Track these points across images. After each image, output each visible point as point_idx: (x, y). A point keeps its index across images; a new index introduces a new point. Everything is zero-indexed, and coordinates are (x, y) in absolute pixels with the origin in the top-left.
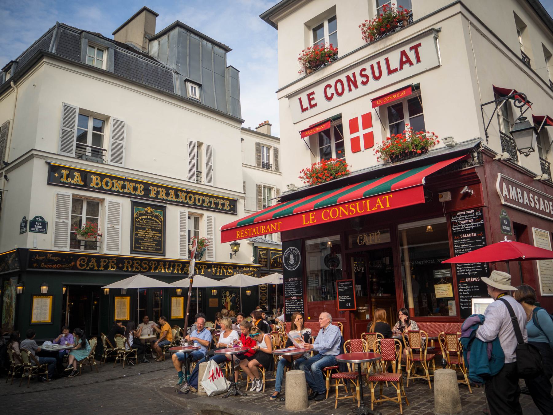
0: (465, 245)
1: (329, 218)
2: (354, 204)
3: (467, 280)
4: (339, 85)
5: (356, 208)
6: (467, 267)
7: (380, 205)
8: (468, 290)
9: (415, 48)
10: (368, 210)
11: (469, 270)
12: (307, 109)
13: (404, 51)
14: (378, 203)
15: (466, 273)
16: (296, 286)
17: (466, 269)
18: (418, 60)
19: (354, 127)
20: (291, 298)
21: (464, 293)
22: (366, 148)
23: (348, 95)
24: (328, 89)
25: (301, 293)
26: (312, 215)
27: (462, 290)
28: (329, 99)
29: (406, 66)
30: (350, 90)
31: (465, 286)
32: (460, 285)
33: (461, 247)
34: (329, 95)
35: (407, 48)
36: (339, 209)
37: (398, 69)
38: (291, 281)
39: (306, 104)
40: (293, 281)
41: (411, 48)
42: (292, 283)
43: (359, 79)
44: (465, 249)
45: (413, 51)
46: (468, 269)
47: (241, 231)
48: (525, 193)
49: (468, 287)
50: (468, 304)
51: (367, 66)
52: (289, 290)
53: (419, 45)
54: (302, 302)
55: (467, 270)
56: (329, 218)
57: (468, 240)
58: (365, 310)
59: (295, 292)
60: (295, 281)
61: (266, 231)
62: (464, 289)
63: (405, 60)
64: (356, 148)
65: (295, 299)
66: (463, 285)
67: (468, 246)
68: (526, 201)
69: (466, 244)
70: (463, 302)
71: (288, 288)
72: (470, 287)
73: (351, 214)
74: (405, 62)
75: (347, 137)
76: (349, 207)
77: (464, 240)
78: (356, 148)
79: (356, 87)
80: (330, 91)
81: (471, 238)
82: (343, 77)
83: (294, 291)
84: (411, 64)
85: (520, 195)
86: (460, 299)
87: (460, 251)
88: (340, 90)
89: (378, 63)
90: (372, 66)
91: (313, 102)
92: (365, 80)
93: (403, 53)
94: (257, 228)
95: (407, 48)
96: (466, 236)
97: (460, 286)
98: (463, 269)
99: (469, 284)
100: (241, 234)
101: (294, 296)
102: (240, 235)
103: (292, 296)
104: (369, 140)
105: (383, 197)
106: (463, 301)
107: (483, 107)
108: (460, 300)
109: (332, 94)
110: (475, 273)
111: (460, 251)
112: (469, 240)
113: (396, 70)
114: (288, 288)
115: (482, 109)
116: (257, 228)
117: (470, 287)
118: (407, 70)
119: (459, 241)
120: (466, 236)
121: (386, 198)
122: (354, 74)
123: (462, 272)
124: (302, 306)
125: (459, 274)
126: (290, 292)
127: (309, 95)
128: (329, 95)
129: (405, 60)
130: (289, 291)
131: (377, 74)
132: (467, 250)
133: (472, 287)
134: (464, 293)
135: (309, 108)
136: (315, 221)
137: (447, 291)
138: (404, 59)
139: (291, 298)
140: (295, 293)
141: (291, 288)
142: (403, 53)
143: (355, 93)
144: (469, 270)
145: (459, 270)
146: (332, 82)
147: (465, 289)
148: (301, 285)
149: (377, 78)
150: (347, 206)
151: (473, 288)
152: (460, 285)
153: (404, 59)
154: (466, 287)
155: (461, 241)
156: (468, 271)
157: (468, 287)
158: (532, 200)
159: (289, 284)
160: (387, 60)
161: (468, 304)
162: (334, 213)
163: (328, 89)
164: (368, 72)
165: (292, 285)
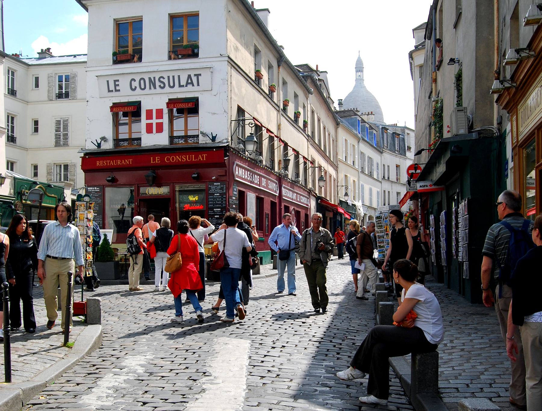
4: (142, 82)
9: (198, 76)
12: (112, 91)
13: (190, 75)
18: (198, 85)
19: (149, 114)
22: (157, 132)
23: (147, 91)
24: (133, 82)
29: (190, 86)
30: (150, 88)
34: (133, 87)
37: (185, 86)
41: (195, 75)
43: (158, 84)
45: (196, 77)
53: (200, 75)
63: (190, 82)
68: (246, 177)
74: (190, 83)
79: (155, 88)
84: (193, 85)
85: (243, 173)
88: (143, 87)
89: (173, 77)
90: (169, 77)
91: (118, 88)
92: (162, 85)
93: (189, 76)
104: (160, 128)
107: (232, 122)
109: (136, 87)
113: (183, 86)
115: (231, 123)
122: (154, 78)
127: (115, 81)
128: (133, 87)
129: (190, 82)
131: (172, 84)
135: (114, 91)
138: (189, 81)
142: (189, 76)
143: (153, 91)
153: (189, 81)
160: (179, 76)
163: (133, 82)
164: (166, 81)
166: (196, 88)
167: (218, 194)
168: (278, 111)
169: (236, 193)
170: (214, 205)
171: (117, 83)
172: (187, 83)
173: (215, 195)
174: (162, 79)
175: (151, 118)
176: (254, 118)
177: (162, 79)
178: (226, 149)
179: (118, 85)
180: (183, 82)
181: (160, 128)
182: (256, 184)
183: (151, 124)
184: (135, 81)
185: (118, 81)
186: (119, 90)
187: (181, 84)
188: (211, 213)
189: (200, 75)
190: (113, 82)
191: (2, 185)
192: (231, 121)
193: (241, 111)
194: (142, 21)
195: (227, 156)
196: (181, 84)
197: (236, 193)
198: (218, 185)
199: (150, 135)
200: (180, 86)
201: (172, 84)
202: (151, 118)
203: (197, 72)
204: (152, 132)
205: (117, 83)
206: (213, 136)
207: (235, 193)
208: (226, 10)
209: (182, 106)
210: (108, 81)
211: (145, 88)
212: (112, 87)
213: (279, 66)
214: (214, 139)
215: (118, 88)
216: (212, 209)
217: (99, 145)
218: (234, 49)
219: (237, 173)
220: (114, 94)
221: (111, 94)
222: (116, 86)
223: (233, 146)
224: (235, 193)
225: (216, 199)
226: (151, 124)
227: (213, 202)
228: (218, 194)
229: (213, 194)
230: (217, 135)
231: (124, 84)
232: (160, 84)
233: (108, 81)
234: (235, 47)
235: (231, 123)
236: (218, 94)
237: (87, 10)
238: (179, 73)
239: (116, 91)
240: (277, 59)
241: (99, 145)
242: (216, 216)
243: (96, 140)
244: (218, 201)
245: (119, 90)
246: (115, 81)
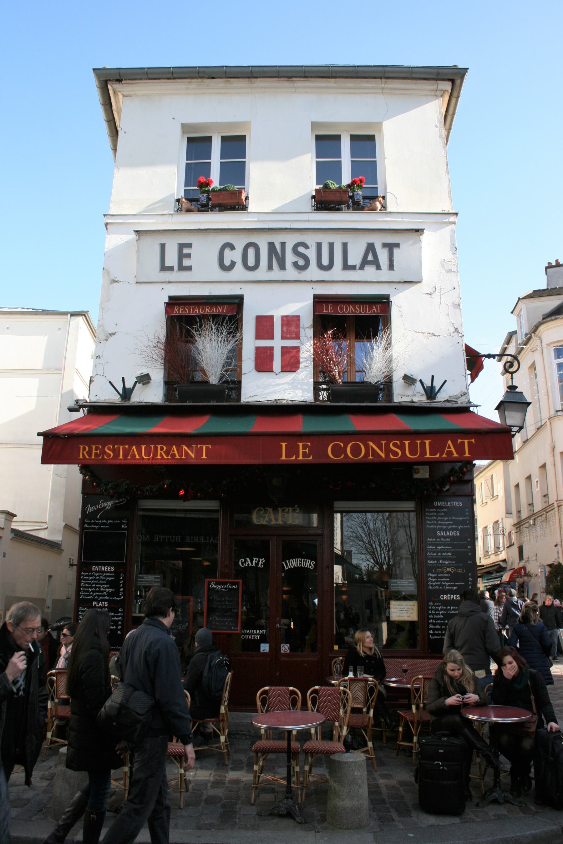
0: (442, 547)
1: (343, 456)
2: (398, 442)
3: (442, 597)
4: (251, 252)
5: (403, 450)
6: (444, 579)
7: (452, 451)
8: (443, 612)
9: (391, 247)
10: (428, 455)
11: (445, 583)
12: (171, 269)
14: (449, 447)
15: (441, 588)
16: (108, 582)
17: (441, 581)
20: (94, 603)
21: (435, 616)
23: (262, 273)
24: (227, 251)
25: (120, 597)
26: (304, 447)
27: (433, 612)
30: (270, 267)
31: (439, 606)
32: (431, 604)
33: (436, 548)
34: (227, 263)
36: (367, 446)
37: (358, 267)
38: (96, 572)
39: (172, 259)
40: (104, 572)
41: (385, 245)
42: (99, 576)
43: (290, 258)
44: (442, 552)
46: (444, 581)
47: (94, 447)
49: (442, 607)
50: (440, 632)
52: (91, 587)
54: (120, 614)
55: (443, 583)
56: (343, 456)
57: (448, 540)
58: (258, 634)
59: (105, 593)
60: (108, 572)
61: (167, 456)
62: (435, 610)
65: (105, 607)
66: (435, 604)
67: (448, 549)
69: (444, 545)
70: (434, 630)
71: (89, 584)
72: (445, 608)
73: (392, 456)
74: (370, 263)
76: (387, 445)
77: (442, 539)
79: (282, 267)
80: (229, 256)
81: (453, 538)
82: (263, 243)
83: (102, 592)
84: (379, 268)
86: (429, 624)
87: (435, 554)
88: (251, 261)
90: (319, 246)
92: (301, 262)
93: (371, 247)
94: (143, 447)
96: (446, 534)
97: (430, 605)
98: (437, 581)
99: (446, 603)
100: (94, 452)
101: (102, 600)
102: (90, 453)
103: (96, 600)
105: (459, 441)
106: (433, 627)
108: (428, 626)
109: (233, 264)
110: (455, 588)
111: (435, 554)
112: (449, 540)
113: (353, 268)
114: (89, 584)
116: (143, 447)
117: (445, 608)
118: (370, 272)
119: (434, 540)
120: (446, 534)
121: (464, 442)
122: (283, 245)
123: (436, 585)
124: (119, 620)
125: (430, 588)
126: (93, 592)
128: (227, 263)
130: (91, 590)
132: (446, 554)
133: (449, 608)
134: (435, 616)
135: (176, 268)
136: (311, 458)
137: (409, 612)
138: (370, 258)
139: (94, 603)
140: (104, 596)
141: (96, 584)
142: (371, 247)
143: (276, 274)
144: (445, 583)
145: (432, 581)
147: (438, 610)
148: (122, 582)
149: (320, 266)
150: (383, 442)
151: (450, 609)
152: (431, 604)
153: (370, 258)
154: (440, 608)
155: (438, 540)
156: (445, 585)
157: (442, 607)
159: (91, 576)
160: (345, 246)
161: (440, 632)
162: (356, 450)
163: (227, 251)
165: (99, 580)
166: (385, 274)
171: (186, 251)
172: (364, 263)
174: (301, 249)
179: (189, 256)
180: (355, 258)
184: (232, 247)
185: (190, 245)
186: (189, 268)
187: (350, 263)
196: (350, 263)
200: (346, 266)
201: (325, 261)
203: (391, 239)
204: (271, 370)
205: (186, 251)
209: (356, 309)
210: (163, 246)
211: (256, 266)
215: (186, 262)
220: (176, 275)
221: (168, 276)
232: (295, 259)
233: (163, 246)
239: (182, 268)
245: (189, 268)
246: (182, 246)
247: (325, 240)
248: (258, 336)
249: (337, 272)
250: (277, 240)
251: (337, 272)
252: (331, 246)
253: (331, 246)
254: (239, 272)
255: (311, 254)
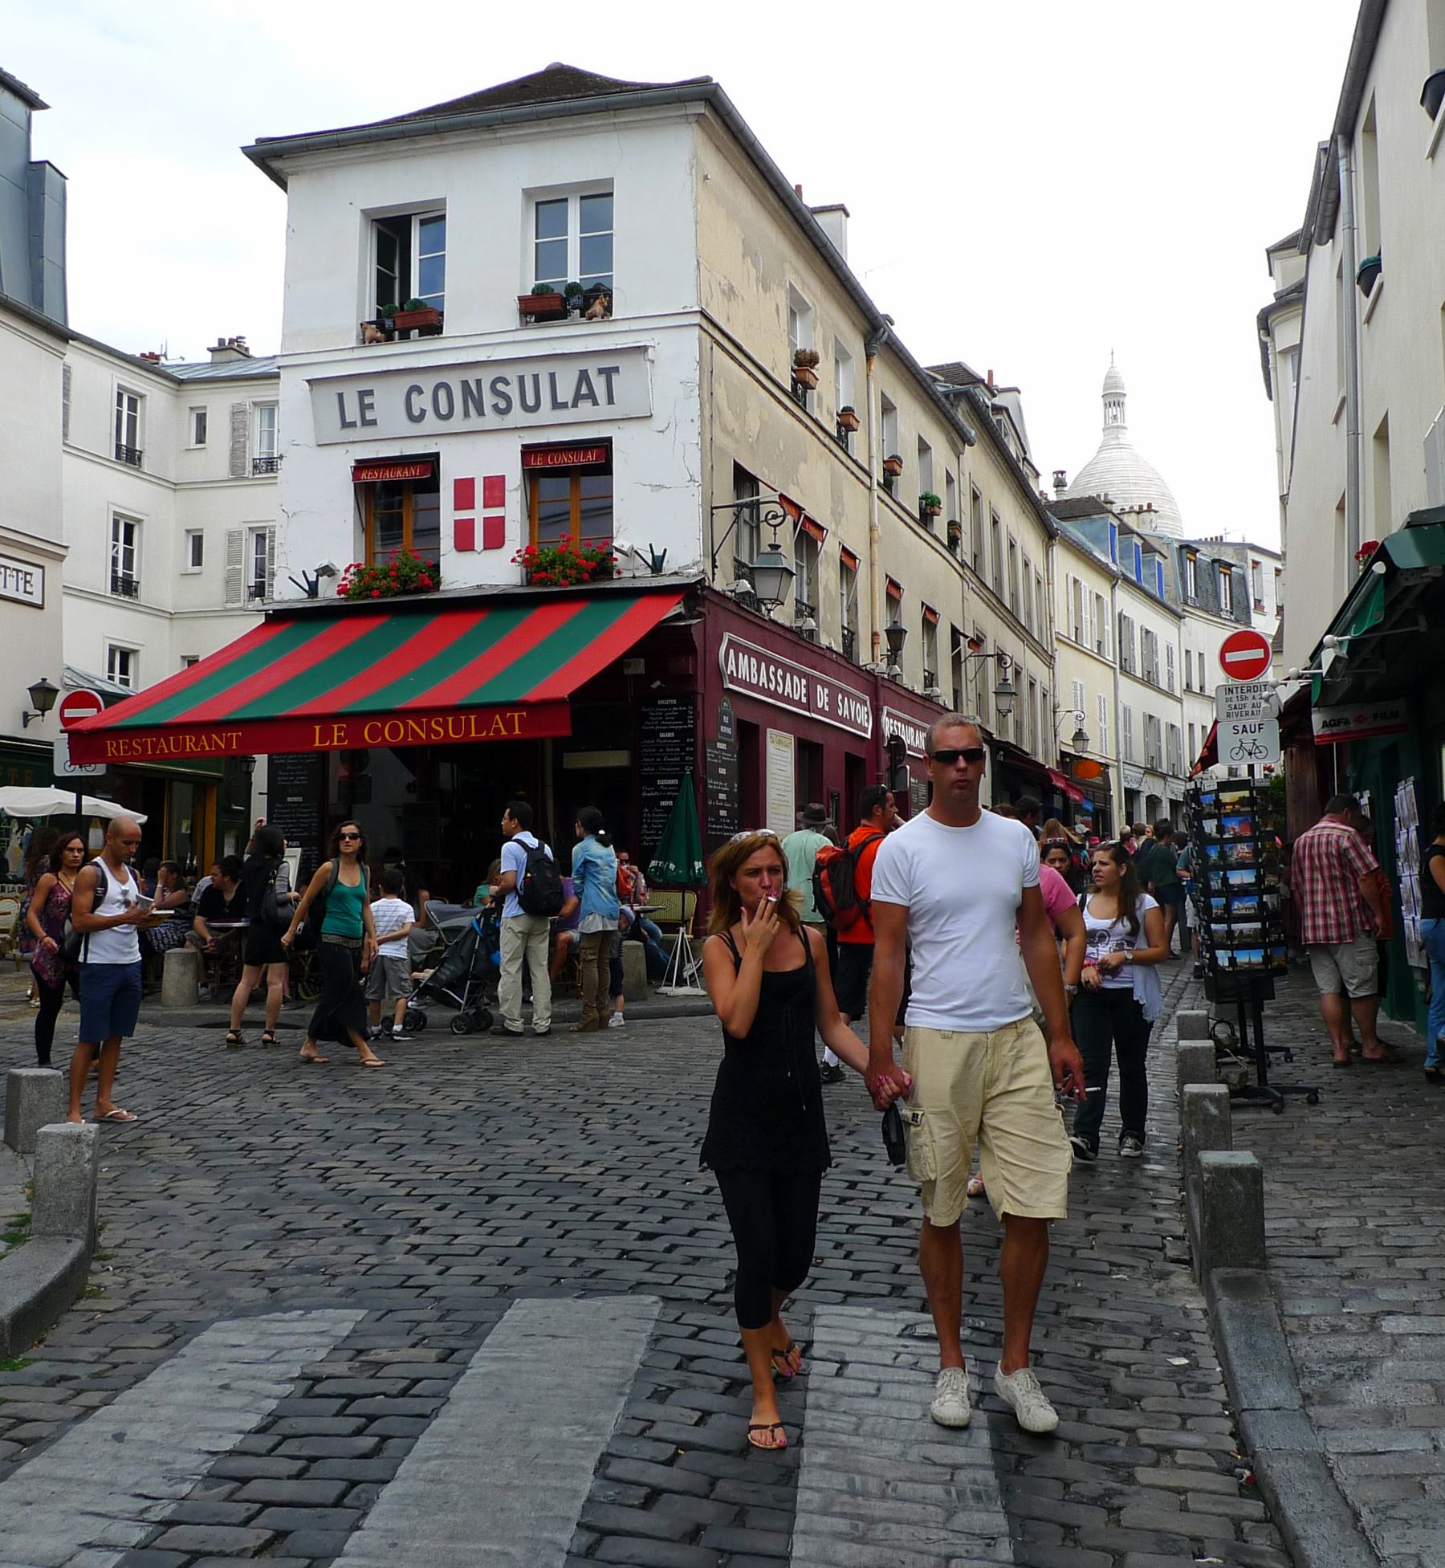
4: (442, 394)
9: (608, 373)
12: (353, 424)
18: (611, 401)
23: (457, 423)
28: (417, 419)
29: (585, 406)
30: (467, 414)
34: (416, 412)
35: (592, 367)
37: (570, 405)
41: (601, 371)
43: (489, 399)
48: (763, 664)
51: (511, 374)
53: (616, 370)
63: (584, 393)
64: (464, 542)
68: (763, 680)
74: (585, 397)
75: (448, 516)
78: (464, 542)
79: (481, 412)
82: (454, 381)
84: (595, 403)
85: (754, 670)
88: (444, 410)
90: (521, 379)
92: (502, 405)
93: (584, 376)
95: (592, 367)
104: (495, 535)
109: (423, 412)
113: (564, 405)
115: (712, 514)
118: (585, 410)
122: (478, 382)
128: (416, 412)
129: (584, 393)
135: (359, 423)
138: (584, 390)
142: (584, 376)
143: (475, 422)
146: (428, 384)
149: (526, 408)
153: (584, 390)
158: (772, 677)
160: (552, 376)
163: (414, 396)
166: (604, 410)
167: (669, 735)
168: (870, 489)
169: (729, 731)
170: (657, 767)
171: (367, 400)
172: (578, 397)
173: (662, 735)
174: (500, 387)
175: (471, 506)
176: (782, 496)
177: (500, 387)
178: (693, 593)
179: (371, 406)
180: (565, 394)
181: (495, 535)
182: (798, 704)
183: (471, 522)
184: (420, 391)
185: (370, 393)
186: (374, 422)
188: (647, 792)
189: (616, 370)
190: (356, 397)
191: (46, 713)
192: (712, 508)
193: (744, 479)
194: (443, 217)
195: (700, 615)
197: (729, 731)
198: (671, 706)
199: (467, 556)
200: (556, 405)
201: (531, 401)
202: (471, 506)
205: (367, 400)
206: (656, 554)
207: (723, 729)
208: (694, 172)
210: (340, 396)
212: (353, 413)
213: (869, 357)
214: (657, 565)
215: (369, 415)
216: (651, 781)
217: (313, 590)
218: (723, 292)
219: (732, 667)
220: (360, 432)
222: (364, 407)
223: (718, 586)
224: (723, 729)
225: (664, 748)
226: (471, 522)
227: (656, 757)
228: (669, 735)
229: (654, 734)
230: (665, 550)
231: (388, 402)
232: (495, 399)
233: (340, 396)
234: (726, 288)
235: (712, 514)
236: (672, 426)
237: (283, 185)
238: (551, 367)
239: (367, 423)
240: (865, 338)
241: (313, 590)
242: (663, 803)
243: (304, 572)
244: (670, 757)
245: (374, 422)
246: (362, 394)
247: (528, 372)
248: (458, 506)
249: (546, 414)
250: (471, 377)
251: (546, 414)
252: (536, 378)
253: (536, 378)
254: (431, 423)
255: (513, 391)
